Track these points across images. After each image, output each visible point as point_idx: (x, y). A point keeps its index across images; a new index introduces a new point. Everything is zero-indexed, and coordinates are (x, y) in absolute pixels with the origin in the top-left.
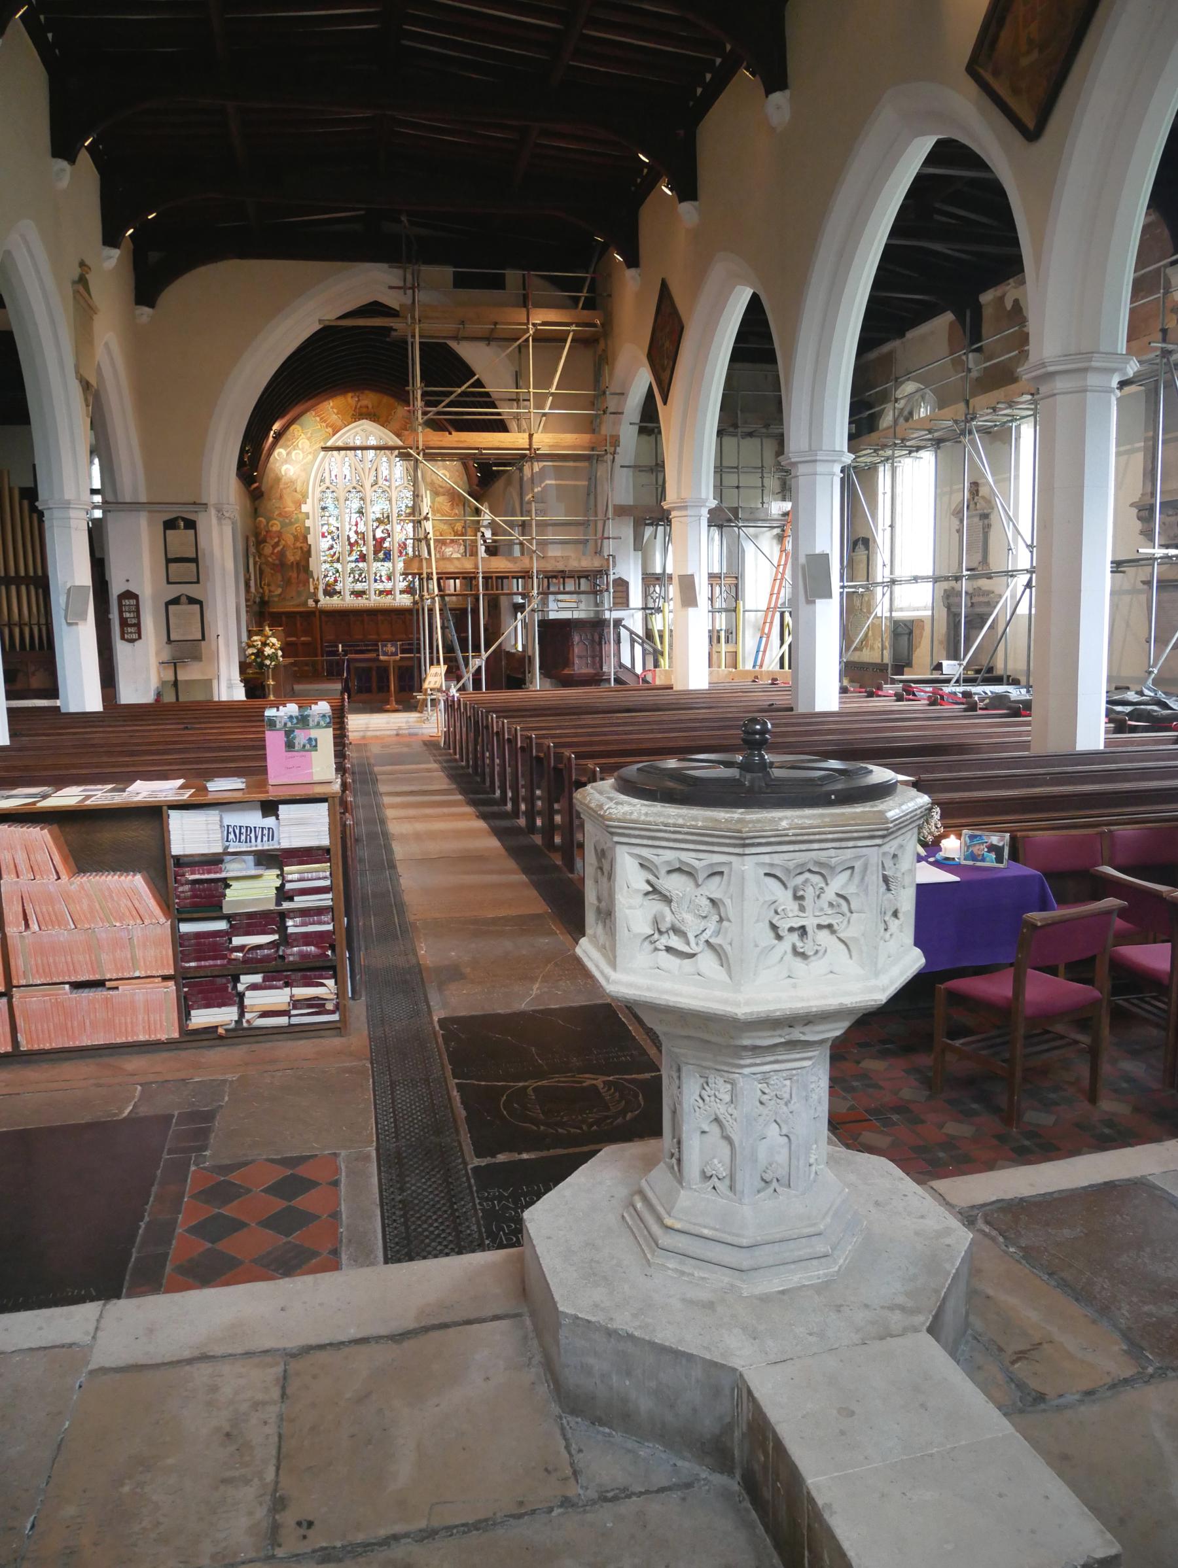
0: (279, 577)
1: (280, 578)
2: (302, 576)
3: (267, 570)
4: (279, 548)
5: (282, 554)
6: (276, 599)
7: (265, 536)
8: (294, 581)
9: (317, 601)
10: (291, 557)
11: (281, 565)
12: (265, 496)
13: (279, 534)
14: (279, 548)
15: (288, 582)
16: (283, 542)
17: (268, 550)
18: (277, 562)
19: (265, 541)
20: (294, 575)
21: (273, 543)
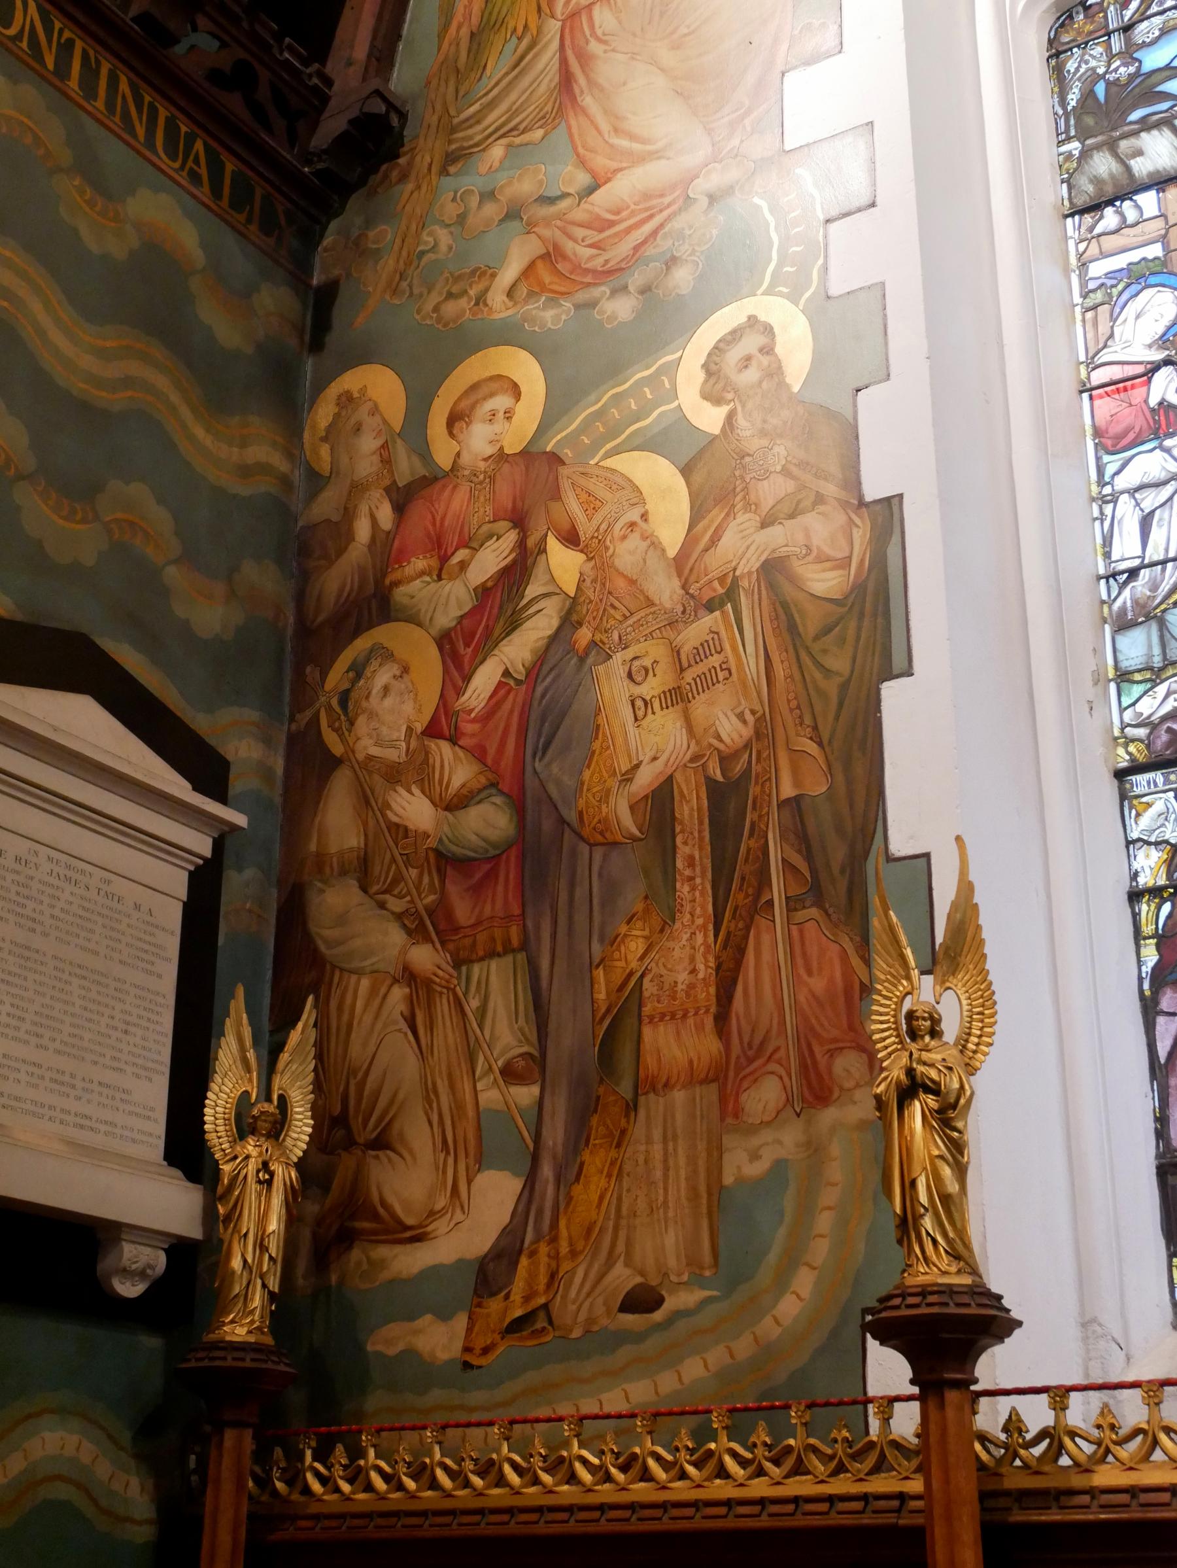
0: (497, 986)
1: (506, 1035)
2: (785, 963)
3: (367, 935)
4: (518, 650)
5: (547, 712)
6: (439, 1339)
7: (388, 552)
8: (674, 1046)
9: (951, 1333)
10: (645, 738)
11: (536, 865)
12: (424, 150)
13: (533, 485)
14: (518, 650)
15: (597, 1078)
16: (563, 564)
17: (392, 703)
18: (488, 822)
19: (375, 604)
20: (682, 958)
21: (450, 600)
